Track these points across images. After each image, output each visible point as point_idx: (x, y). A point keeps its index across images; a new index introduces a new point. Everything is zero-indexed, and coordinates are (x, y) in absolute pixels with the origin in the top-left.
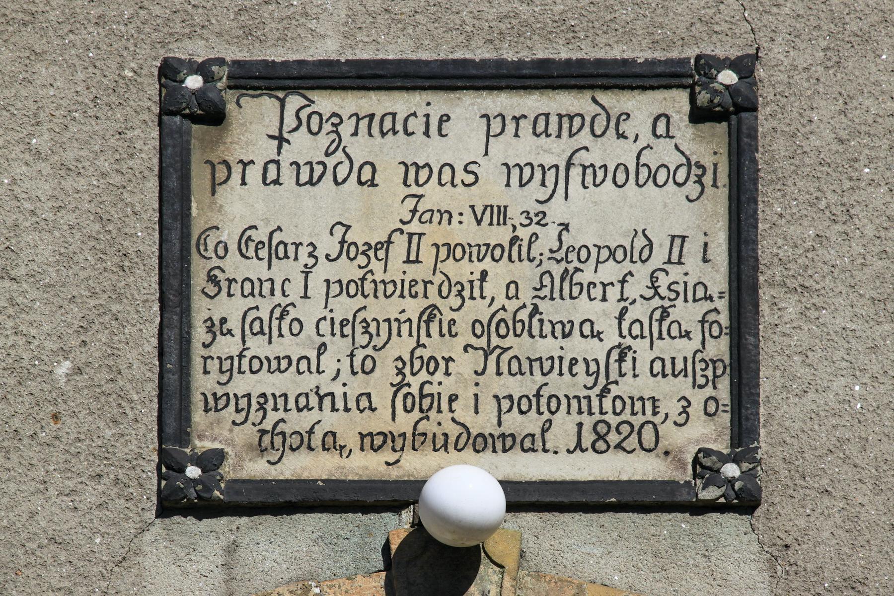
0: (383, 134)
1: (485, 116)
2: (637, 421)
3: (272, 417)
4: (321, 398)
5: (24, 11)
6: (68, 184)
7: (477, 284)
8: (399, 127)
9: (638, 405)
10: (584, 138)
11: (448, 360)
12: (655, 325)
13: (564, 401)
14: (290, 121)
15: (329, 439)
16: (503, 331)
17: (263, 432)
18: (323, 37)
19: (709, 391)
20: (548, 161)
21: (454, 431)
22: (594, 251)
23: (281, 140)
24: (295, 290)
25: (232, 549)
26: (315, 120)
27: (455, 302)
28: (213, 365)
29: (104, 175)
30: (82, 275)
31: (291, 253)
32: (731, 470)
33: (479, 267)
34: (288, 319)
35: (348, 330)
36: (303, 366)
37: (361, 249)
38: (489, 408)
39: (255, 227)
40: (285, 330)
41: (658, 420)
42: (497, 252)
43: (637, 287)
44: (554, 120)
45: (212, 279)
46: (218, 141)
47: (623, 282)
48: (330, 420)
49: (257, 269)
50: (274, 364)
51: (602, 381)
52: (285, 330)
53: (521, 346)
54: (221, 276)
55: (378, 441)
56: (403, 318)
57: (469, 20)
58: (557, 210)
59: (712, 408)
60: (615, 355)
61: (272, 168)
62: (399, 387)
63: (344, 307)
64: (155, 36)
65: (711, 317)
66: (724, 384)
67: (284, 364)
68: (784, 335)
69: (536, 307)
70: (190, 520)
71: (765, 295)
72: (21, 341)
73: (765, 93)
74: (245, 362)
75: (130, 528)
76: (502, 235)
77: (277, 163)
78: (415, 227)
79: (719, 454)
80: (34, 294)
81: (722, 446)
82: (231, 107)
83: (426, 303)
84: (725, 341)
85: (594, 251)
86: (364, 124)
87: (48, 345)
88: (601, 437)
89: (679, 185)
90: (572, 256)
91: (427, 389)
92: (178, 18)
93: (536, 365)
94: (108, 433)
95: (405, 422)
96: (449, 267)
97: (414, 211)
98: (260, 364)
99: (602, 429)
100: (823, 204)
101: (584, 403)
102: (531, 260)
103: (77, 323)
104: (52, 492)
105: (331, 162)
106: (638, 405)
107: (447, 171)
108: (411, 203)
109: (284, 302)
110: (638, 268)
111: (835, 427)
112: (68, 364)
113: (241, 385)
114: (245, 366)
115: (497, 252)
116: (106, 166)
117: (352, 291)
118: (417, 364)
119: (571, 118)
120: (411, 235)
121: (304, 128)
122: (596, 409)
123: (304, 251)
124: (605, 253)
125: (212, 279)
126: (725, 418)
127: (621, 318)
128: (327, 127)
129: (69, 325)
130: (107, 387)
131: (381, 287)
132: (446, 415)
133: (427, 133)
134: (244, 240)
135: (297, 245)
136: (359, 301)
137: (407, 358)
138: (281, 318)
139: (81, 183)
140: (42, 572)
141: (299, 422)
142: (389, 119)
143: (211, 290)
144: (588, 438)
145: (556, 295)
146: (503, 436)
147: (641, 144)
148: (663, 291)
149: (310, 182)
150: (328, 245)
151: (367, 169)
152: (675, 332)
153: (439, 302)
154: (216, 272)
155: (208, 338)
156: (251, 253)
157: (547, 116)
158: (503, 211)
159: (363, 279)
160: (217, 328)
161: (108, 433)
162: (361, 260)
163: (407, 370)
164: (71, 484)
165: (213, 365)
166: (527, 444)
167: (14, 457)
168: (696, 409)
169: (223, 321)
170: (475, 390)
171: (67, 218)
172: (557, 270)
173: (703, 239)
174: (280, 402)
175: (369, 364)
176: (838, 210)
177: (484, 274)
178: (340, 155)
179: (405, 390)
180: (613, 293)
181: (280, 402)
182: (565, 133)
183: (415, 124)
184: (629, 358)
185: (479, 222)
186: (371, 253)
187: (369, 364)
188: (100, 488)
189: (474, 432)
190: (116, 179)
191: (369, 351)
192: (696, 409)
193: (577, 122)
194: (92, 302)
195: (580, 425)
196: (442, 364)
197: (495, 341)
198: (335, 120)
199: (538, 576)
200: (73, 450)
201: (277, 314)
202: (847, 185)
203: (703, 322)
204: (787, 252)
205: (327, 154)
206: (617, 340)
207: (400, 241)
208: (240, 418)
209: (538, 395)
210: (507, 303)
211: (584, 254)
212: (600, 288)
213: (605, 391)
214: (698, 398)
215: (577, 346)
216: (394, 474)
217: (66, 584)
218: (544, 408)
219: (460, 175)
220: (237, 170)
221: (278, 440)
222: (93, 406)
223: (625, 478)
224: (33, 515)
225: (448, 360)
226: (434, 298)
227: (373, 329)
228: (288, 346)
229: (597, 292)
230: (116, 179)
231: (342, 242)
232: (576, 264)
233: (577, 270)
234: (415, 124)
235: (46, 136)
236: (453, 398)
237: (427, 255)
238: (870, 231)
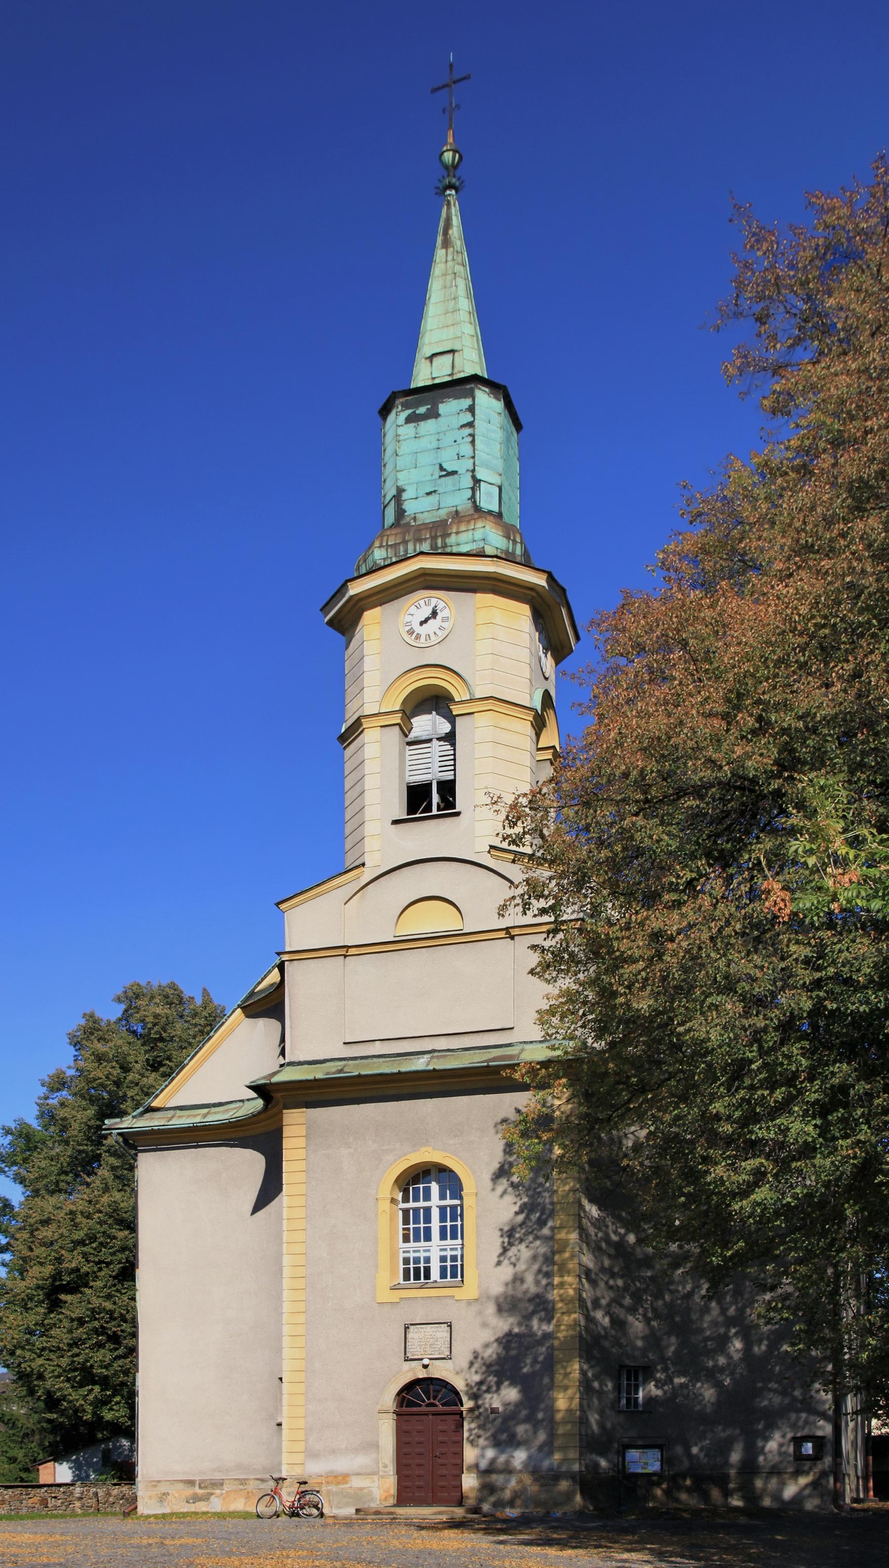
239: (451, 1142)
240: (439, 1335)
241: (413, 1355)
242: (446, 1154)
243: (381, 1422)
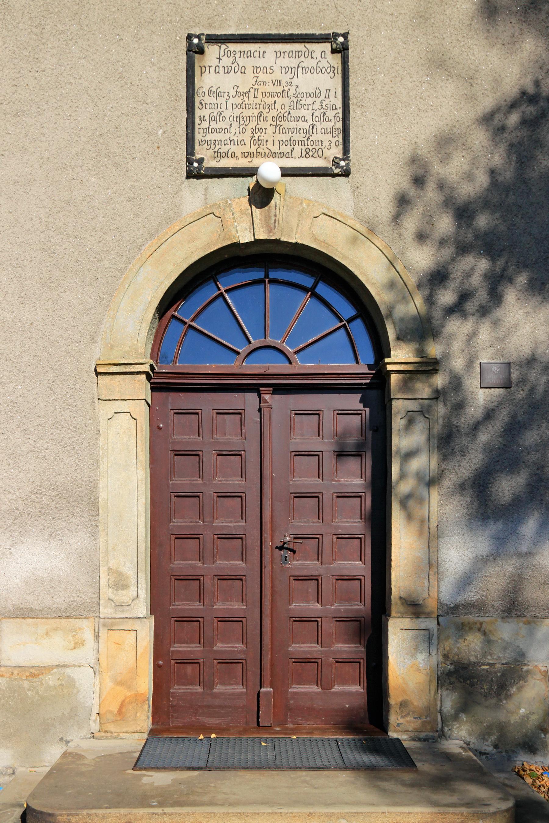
0: (248, 57)
1: (276, 52)
2: (317, 148)
3: (217, 147)
4: (231, 141)
5: (150, 19)
6: (162, 73)
7: (273, 105)
8: (252, 55)
9: (317, 143)
10: (302, 58)
11: (266, 129)
12: (322, 117)
13: (297, 142)
14: (222, 53)
15: (233, 154)
16: (280, 120)
17: (215, 152)
18: (231, 26)
19: (336, 138)
20: (293, 66)
21: (267, 151)
22: (305, 94)
23: (220, 59)
24: (224, 107)
25: (206, 189)
26: (229, 52)
27: (267, 110)
28: (201, 131)
29: (171, 71)
30: (166, 102)
31: (222, 95)
32: (342, 163)
33: (274, 99)
34: (222, 116)
35: (238, 119)
36: (226, 131)
37: (242, 93)
38: (277, 143)
39: (212, 87)
40: (221, 120)
41: (323, 147)
42: (279, 94)
43: (317, 106)
44: (294, 53)
45: (201, 103)
46: (201, 60)
47: (313, 104)
48: (233, 148)
49: (213, 100)
50: (218, 130)
51: (308, 135)
52: (221, 120)
54: (203, 103)
55: (246, 154)
56: (253, 115)
57: (271, 21)
58: (295, 81)
59: (337, 144)
60: (311, 127)
61: (217, 68)
62: (252, 137)
63: (237, 112)
64: (186, 26)
65: (337, 115)
66: (341, 136)
67: (221, 130)
68: (357, 120)
69: (289, 112)
70: (195, 180)
71: (351, 108)
72: (149, 123)
73: (351, 45)
74: (210, 130)
75: (178, 182)
76: (280, 89)
77: (219, 66)
78: (256, 87)
79: (339, 158)
80: (153, 108)
81: (340, 156)
82: (206, 49)
83: (259, 111)
84: (341, 122)
85: (305, 94)
86: (242, 54)
87: (156, 124)
88: (307, 153)
89: (328, 73)
90: (299, 96)
91: (260, 138)
92: (192, 21)
93: (290, 130)
94: (173, 152)
95: (254, 149)
96: (266, 99)
97: (256, 82)
98: (214, 131)
99: (308, 150)
100: (367, 79)
101: (303, 142)
102: (288, 97)
103: (164, 118)
104: (157, 171)
105: (233, 66)
106: (317, 143)
107: (265, 69)
108: (255, 79)
109: (221, 110)
110: (317, 100)
111: (370, 149)
112: (161, 130)
113: (209, 137)
114: (210, 131)
115: (279, 94)
116: (172, 68)
117: (239, 107)
118: (257, 130)
119: (299, 52)
120: (255, 89)
121: (226, 55)
122: (306, 144)
123: (226, 94)
124: (308, 95)
125: (201, 103)
126: (341, 147)
127: (313, 115)
128: (232, 55)
129: (162, 118)
130: (172, 138)
131: (247, 106)
132: (265, 146)
133: (259, 57)
134: (210, 91)
135: (224, 93)
136: (241, 110)
137: (254, 128)
138: (220, 116)
139: (165, 73)
140: (155, 197)
141: (224, 149)
142: (249, 52)
143: (201, 107)
144: (304, 153)
145: (295, 108)
146: (281, 153)
147: (318, 60)
148: (324, 107)
149: (228, 72)
150: (233, 93)
151: (243, 68)
152: (327, 120)
153: (263, 110)
154: (202, 101)
155: (200, 122)
156: (212, 95)
157: (292, 51)
158: (280, 82)
159: (242, 103)
160: (202, 119)
161: (173, 152)
162: (242, 97)
163: (254, 132)
164: (162, 169)
165: (201, 131)
166: (287, 156)
167: (147, 160)
168: (333, 144)
169: (204, 117)
170: (273, 138)
171: (161, 84)
172: (295, 101)
173: (334, 90)
174: (220, 142)
175: (244, 130)
176: (371, 81)
177: (275, 102)
178: (236, 63)
179: (254, 138)
180: (311, 107)
181: (220, 142)
182: (297, 57)
183: (257, 54)
184: (315, 128)
185: (274, 85)
186: (244, 95)
187: (244, 130)
188: (170, 170)
189: (273, 152)
190: (175, 72)
191: (244, 126)
192: (333, 144)
193: (300, 53)
194: (168, 111)
195: (302, 149)
196: (264, 130)
197: (278, 123)
198: (234, 53)
199: (290, 197)
200: (163, 158)
201: (218, 115)
202: (373, 73)
203: (335, 116)
204: (357, 94)
205: (232, 64)
206: (312, 122)
207: (252, 91)
208: (208, 147)
209: (290, 140)
210: (282, 111)
211: (302, 95)
212: (307, 106)
213: (308, 138)
214: (334, 140)
215: (301, 125)
216: (251, 165)
217: (161, 200)
218: (292, 144)
219: (269, 70)
220: (208, 68)
221: (219, 154)
222: (168, 144)
223: (314, 166)
224: (152, 178)
225: (266, 129)
226: (262, 109)
227: (245, 119)
228: (222, 125)
229: (306, 107)
230: (175, 72)
231: (237, 91)
232: (300, 98)
233: (301, 100)
234: (257, 54)
235: (156, 58)
236: (267, 141)
237: (260, 95)
238: (379, 88)
241: (217, 155)
243: (108, 409)
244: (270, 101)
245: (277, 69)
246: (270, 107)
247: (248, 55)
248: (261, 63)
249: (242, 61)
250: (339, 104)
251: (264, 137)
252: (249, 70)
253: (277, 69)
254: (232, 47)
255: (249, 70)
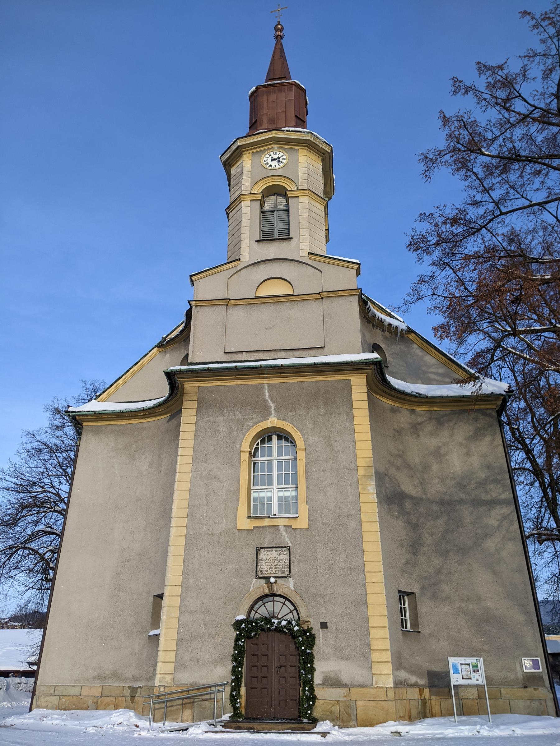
53: (277, 567)
113: (261, 570)
141: (264, 572)
215: (280, 567)
228: (263, 567)
239: (288, 414)
240: (281, 557)
242: (285, 422)
244: (273, 561)
245: (275, 554)
246: (274, 563)
247: (269, 551)
248: (271, 553)
249: (268, 553)
250: (288, 562)
251: (272, 570)
252: (269, 555)
253: (275, 554)
254: (266, 549)
255: (269, 555)
